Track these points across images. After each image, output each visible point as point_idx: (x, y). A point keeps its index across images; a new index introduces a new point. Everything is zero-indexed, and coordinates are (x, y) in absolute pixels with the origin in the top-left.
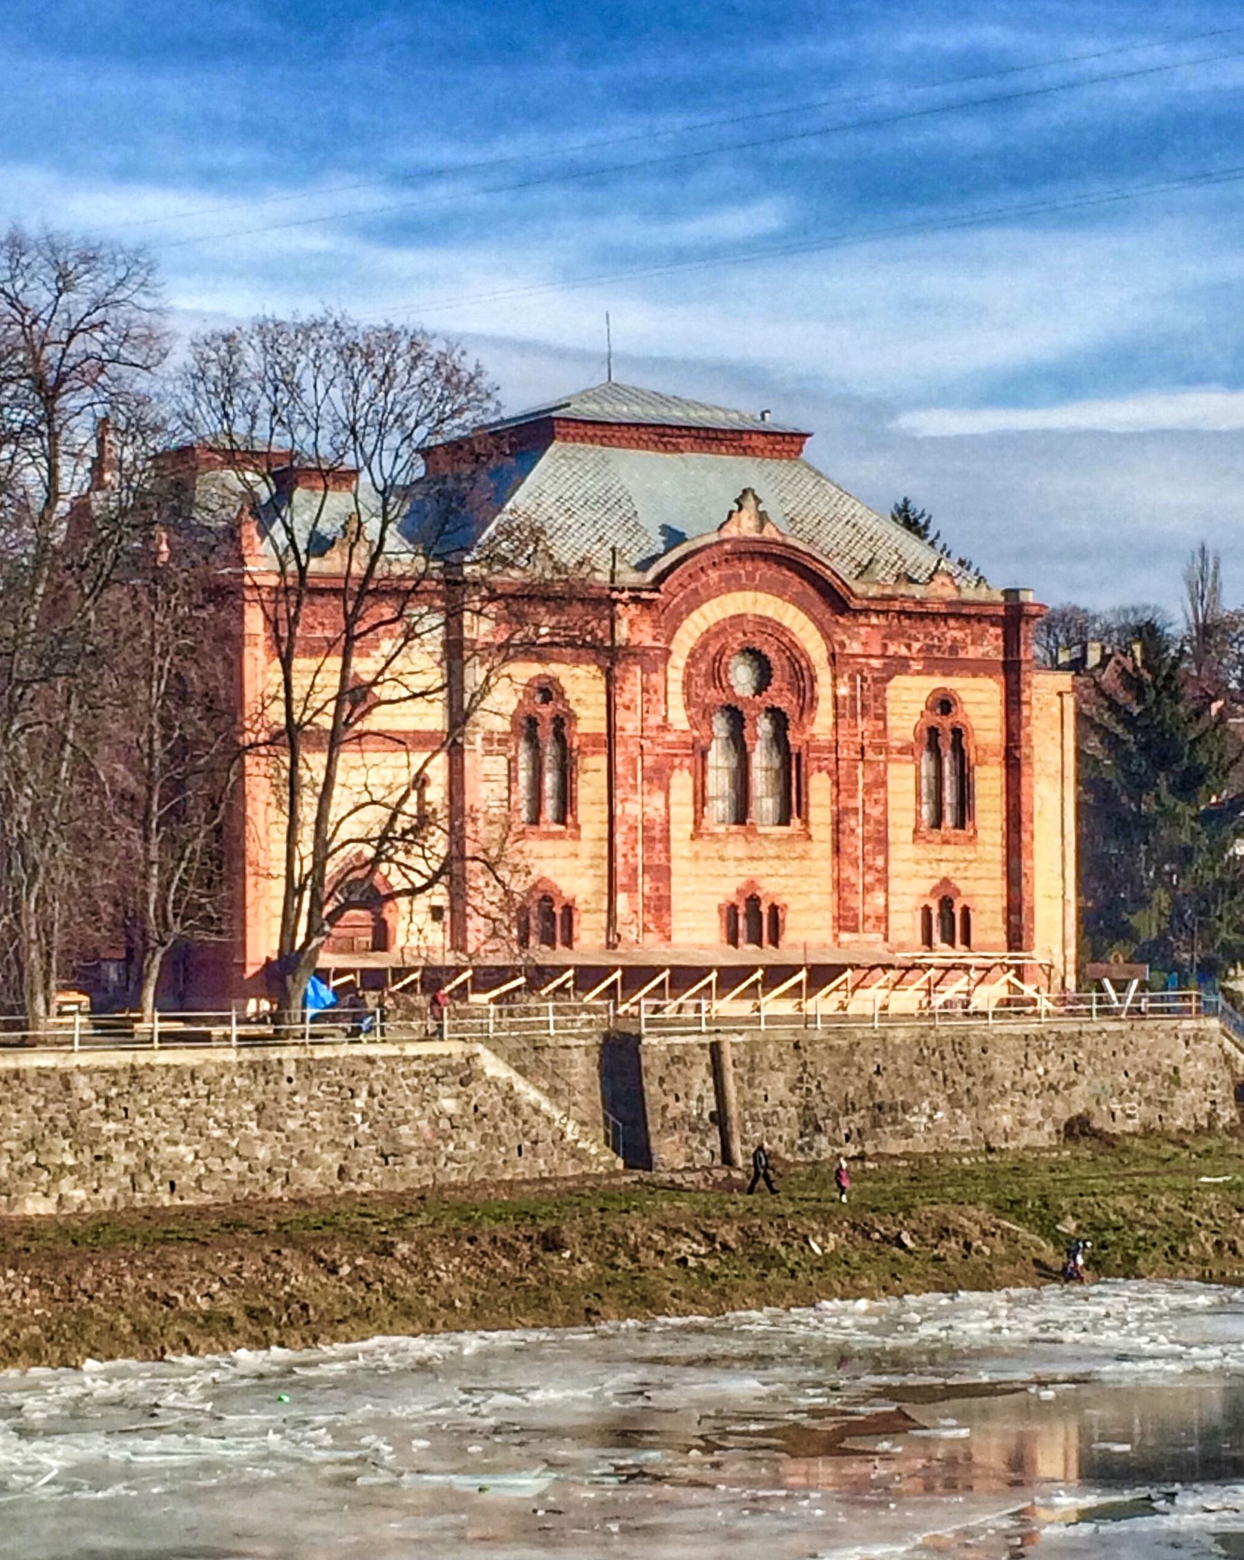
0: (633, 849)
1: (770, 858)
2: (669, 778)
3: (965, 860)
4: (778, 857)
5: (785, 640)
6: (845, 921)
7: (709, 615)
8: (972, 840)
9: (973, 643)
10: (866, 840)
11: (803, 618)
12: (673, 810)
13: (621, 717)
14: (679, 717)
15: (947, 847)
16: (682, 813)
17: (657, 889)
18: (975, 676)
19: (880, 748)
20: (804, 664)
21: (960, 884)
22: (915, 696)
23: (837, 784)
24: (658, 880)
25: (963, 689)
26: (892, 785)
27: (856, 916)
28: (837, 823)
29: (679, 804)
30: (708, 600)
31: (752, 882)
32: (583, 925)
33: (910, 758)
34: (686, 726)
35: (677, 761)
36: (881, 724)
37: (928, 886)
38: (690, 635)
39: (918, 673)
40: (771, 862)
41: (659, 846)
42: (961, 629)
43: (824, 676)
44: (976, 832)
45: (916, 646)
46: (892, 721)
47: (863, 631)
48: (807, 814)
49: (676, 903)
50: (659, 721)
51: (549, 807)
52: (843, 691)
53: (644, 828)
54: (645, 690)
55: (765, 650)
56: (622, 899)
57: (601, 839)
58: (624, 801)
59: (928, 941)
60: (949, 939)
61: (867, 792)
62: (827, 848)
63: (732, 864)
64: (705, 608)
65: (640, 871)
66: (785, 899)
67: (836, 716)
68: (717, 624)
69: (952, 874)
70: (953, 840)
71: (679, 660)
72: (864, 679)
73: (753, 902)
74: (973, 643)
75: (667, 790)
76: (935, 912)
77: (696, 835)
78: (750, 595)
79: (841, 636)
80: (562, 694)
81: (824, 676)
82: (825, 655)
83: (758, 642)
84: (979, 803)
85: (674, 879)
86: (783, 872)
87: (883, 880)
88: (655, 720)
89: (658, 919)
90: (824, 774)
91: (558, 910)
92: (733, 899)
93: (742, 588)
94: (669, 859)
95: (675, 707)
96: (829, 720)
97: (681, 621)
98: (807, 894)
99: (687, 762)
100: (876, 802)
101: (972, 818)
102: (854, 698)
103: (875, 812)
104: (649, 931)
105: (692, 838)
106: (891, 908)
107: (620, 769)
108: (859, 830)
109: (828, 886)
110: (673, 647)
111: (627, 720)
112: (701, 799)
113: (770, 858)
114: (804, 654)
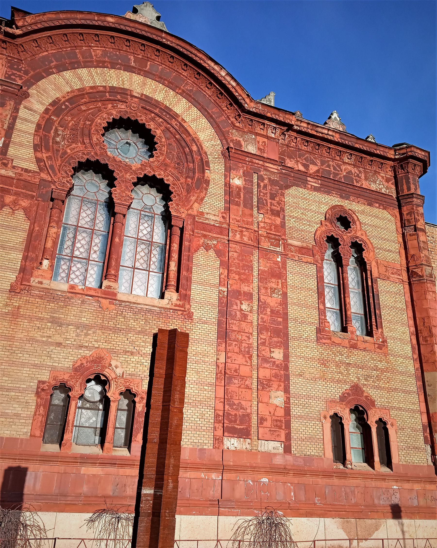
5: (174, 123)
9: (366, 179)
11: (195, 112)
18: (370, 205)
20: (195, 148)
25: (363, 212)
30: (88, 64)
33: (310, 259)
34: (33, 167)
35: (8, 199)
36: (278, 221)
39: (316, 189)
46: (290, 223)
47: (259, 138)
55: (151, 126)
61: (260, 280)
63: (72, 333)
64: (83, 72)
70: (361, 345)
72: (261, 178)
78: (137, 79)
79: (235, 135)
82: (219, 148)
83: (142, 119)
90: (212, 253)
92: (66, 377)
93: (128, 69)
95: (21, 145)
96: (221, 205)
99: (25, 203)
100: (273, 290)
105: (13, 290)
110: (32, 91)
114: (195, 141)
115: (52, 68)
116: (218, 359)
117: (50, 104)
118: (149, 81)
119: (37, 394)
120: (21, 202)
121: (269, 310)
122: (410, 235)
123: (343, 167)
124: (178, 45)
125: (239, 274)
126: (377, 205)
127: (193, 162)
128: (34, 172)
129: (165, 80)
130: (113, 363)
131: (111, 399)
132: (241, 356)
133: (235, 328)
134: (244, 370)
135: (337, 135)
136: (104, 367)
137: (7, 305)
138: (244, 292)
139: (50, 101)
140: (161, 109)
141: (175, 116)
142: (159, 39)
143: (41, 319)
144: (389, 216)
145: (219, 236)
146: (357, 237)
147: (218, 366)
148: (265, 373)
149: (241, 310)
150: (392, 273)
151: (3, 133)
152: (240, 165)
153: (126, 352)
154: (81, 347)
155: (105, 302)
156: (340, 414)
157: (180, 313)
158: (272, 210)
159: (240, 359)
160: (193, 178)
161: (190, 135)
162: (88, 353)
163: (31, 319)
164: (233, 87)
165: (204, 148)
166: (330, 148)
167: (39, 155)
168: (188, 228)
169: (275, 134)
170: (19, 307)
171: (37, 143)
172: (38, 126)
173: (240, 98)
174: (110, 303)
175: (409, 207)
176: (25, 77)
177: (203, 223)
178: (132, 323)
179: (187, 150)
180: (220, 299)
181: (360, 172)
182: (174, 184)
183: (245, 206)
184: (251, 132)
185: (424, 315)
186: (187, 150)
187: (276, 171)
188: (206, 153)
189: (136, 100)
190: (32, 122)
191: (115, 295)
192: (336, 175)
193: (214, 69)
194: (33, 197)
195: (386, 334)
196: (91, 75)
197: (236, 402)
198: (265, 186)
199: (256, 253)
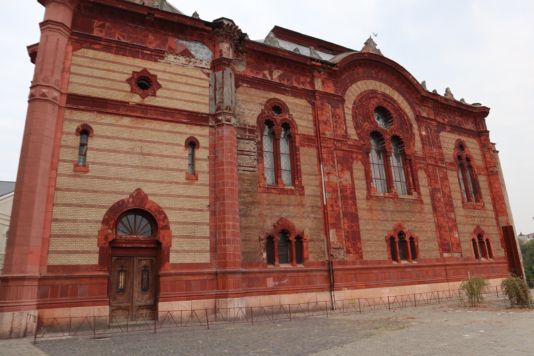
0: (336, 202)
1: (406, 211)
2: (352, 163)
3: (483, 217)
4: (410, 212)
5: (396, 105)
6: (445, 247)
7: (361, 87)
8: (483, 206)
9: (465, 123)
10: (446, 205)
12: (356, 182)
13: (322, 126)
14: (352, 132)
15: (476, 210)
16: (360, 184)
17: (352, 227)
18: (469, 137)
19: (442, 160)
21: (483, 228)
22: (450, 142)
23: (429, 176)
24: (352, 221)
26: (451, 179)
27: (448, 243)
28: (433, 196)
29: (358, 179)
31: (400, 226)
32: (309, 250)
34: (357, 138)
35: (355, 155)
37: (472, 229)
38: (354, 95)
39: (449, 132)
40: (408, 214)
41: (350, 202)
42: (460, 117)
43: (415, 126)
44: (484, 204)
45: (446, 120)
46: (445, 151)
48: (419, 190)
49: (364, 236)
50: (343, 132)
51: (286, 178)
52: (424, 133)
53: (341, 191)
54: (334, 116)
56: (332, 232)
57: (317, 196)
58: (328, 174)
59: (477, 257)
60: (484, 256)
61: (442, 181)
62: (430, 207)
65: (341, 216)
66: (416, 234)
67: (423, 144)
68: (365, 92)
69: (480, 224)
70: (477, 207)
71: (349, 105)
72: (431, 130)
73: (401, 234)
74: (465, 123)
75: (350, 169)
76: (477, 241)
77: (369, 197)
78: (378, 83)
79: (418, 109)
80: (287, 111)
81: (415, 126)
84: (482, 191)
85: (360, 221)
86: (413, 219)
87: (456, 226)
88: (340, 132)
89: (354, 245)
90: (423, 171)
91: (292, 238)
92: (392, 234)
93: (374, 79)
94: (356, 209)
97: (349, 87)
98: (426, 231)
99: (360, 157)
101: (481, 197)
102: (429, 138)
103: (447, 191)
104: (351, 253)
105: (367, 199)
106: (461, 239)
107: (325, 156)
108: (442, 200)
109: (433, 227)
110: (346, 98)
111: (325, 130)
112: (368, 178)
113: (406, 211)
114: (405, 113)
115: (348, 84)
116: (435, 220)
117: (353, 104)
118: (382, 83)
119: (386, 242)
120: (359, 157)
121: (446, 195)
122: (486, 151)
123: (456, 118)
124: (392, 64)
125: (434, 179)
126: (471, 137)
127: (407, 125)
128: (359, 141)
129: (387, 82)
130: (405, 226)
131: (407, 241)
132: (442, 218)
133: (438, 206)
134: (444, 224)
135: (455, 103)
136: (402, 228)
137: (367, 205)
138: (438, 188)
139: (353, 102)
140: (389, 98)
141: (395, 102)
142: (384, 62)
143: (379, 210)
144: (476, 142)
145: (424, 162)
146: (468, 155)
147: (435, 223)
148: (451, 224)
149: (438, 197)
150: (482, 171)
151: (343, 122)
152: (423, 124)
153: (407, 221)
154: (393, 220)
155: (395, 199)
156: (474, 238)
157: (419, 201)
158: (438, 146)
159: (442, 219)
160: (408, 133)
161: (403, 111)
162: (396, 223)
163: (376, 210)
164: (415, 84)
165: (410, 118)
166: (451, 109)
167: (357, 132)
168: (413, 159)
169: (431, 105)
170: (371, 206)
171: (355, 125)
172: (353, 116)
173: (419, 89)
174: (397, 200)
175: (484, 137)
176: (341, 91)
177: (417, 156)
178: (406, 208)
179: (403, 119)
180: (430, 193)
181: (462, 119)
182: (403, 138)
183: (429, 146)
184: (423, 106)
185: (496, 190)
186: (403, 119)
187: (435, 125)
188: (410, 119)
189: (380, 95)
190: (350, 115)
191: (397, 196)
192: (455, 122)
193: (407, 75)
194: (361, 153)
195: (484, 201)
196: (362, 85)
197: (444, 238)
198: (433, 133)
199: (437, 168)
